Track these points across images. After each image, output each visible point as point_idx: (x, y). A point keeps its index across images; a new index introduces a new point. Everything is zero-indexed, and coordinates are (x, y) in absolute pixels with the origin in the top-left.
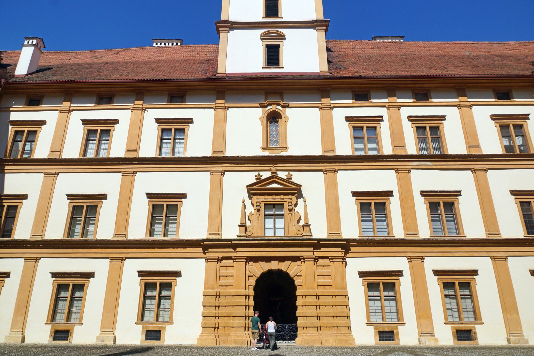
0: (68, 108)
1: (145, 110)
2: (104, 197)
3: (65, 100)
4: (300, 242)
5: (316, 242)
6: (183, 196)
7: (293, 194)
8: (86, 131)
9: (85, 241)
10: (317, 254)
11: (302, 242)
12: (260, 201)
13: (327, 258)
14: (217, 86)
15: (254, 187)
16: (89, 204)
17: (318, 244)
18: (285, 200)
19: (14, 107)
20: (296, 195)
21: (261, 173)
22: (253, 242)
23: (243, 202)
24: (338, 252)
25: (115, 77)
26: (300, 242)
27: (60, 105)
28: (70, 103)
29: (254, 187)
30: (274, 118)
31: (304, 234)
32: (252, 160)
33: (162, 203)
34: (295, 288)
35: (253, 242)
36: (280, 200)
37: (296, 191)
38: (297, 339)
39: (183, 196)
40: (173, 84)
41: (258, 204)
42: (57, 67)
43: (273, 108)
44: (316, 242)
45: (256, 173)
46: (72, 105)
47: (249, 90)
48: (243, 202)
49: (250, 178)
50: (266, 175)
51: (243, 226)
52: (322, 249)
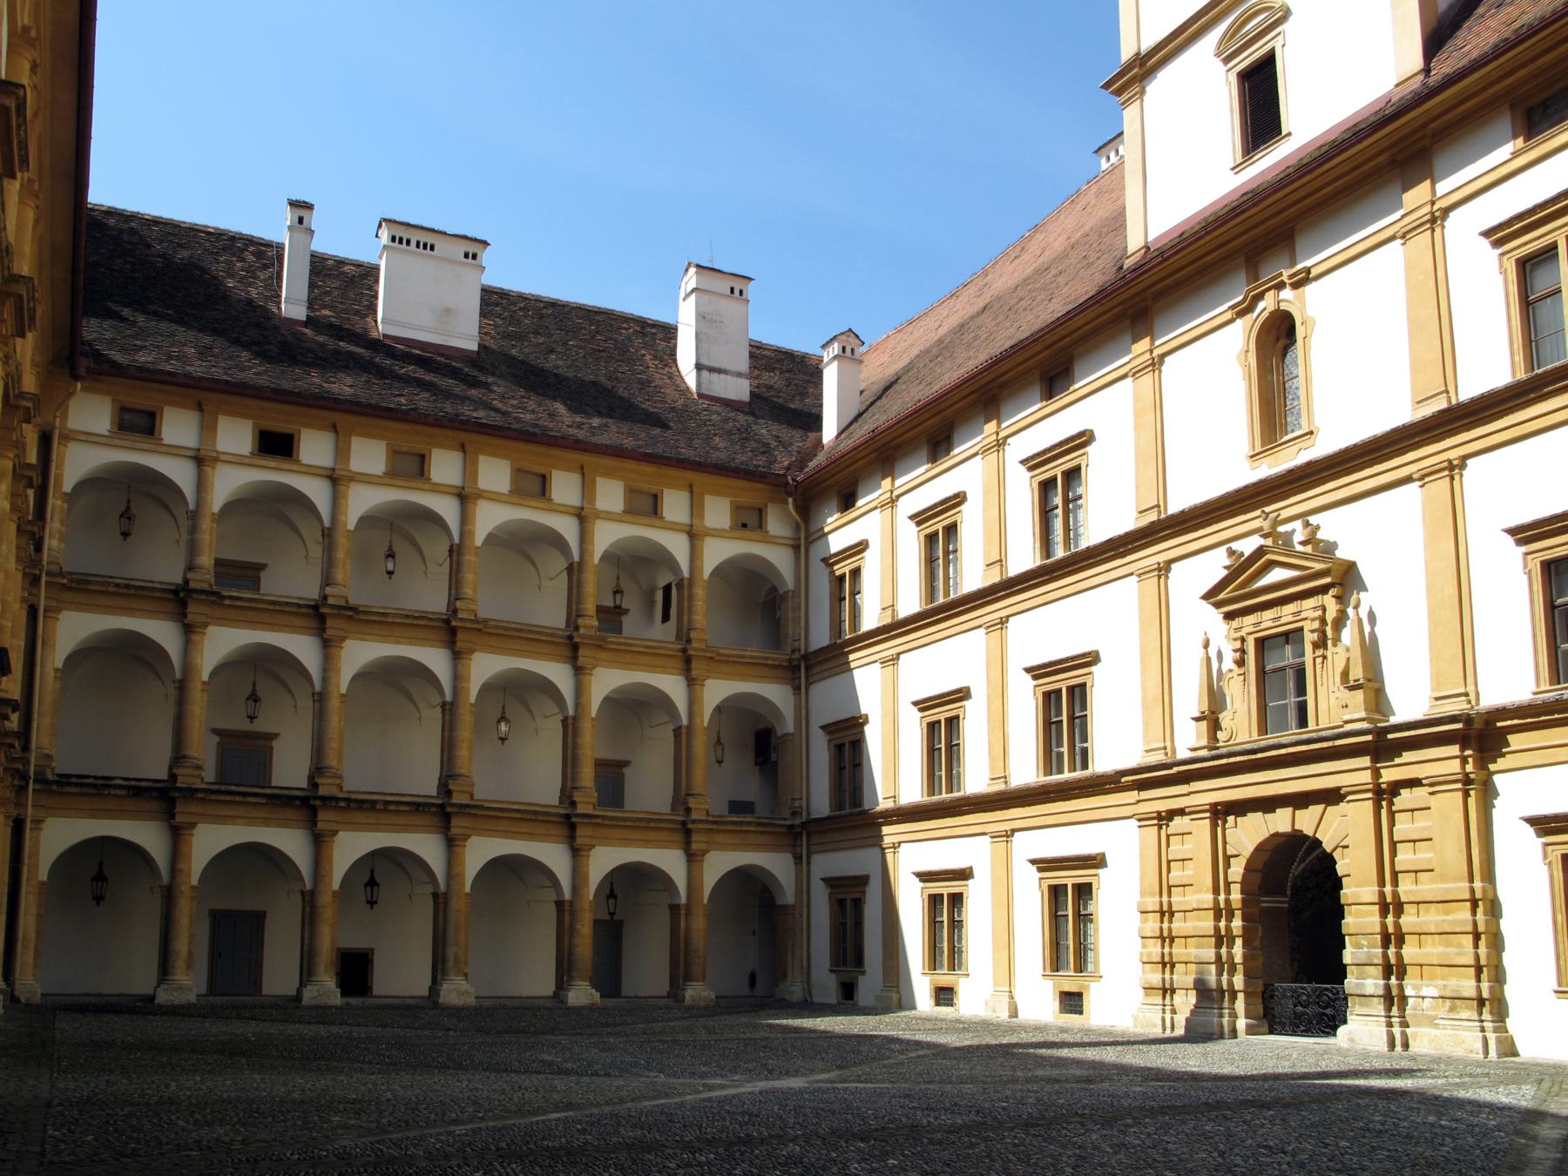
0: (1147, 356)
1: (1004, 444)
2: (962, 694)
3: (1135, 341)
4: (1325, 745)
5: (1369, 738)
6: (1091, 659)
7: (1323, 590)
8: (1035, 485)
9: (958, 799)
10: (1389, 775)
11: (1330, 744)
12: (1243, 633)
13: (1414, 783)
14: (1126, 300)
15: (1221, 596)
16: (948, 715)
17: (1383, 744)
18: (1303, 615)
19: (832, 520)
20: (1332, 592)
21: (1235, 546)
22: (1232, 760)
23: (1206, 646)
24: (1445, 761)
25: (1056, 308)
26: (1325, 745)
27: (979, 439)
28: (1148, 339)
29: (1221, 596)
30: (1279, 335)
31: (1346, 717)
32: (1232, 504)
33: (1056, 686)
34: (1337, 884)
35: (1232, 760)
36: (1290, 618)
37: (1328, 580)
38: (1341, 1030)
39: (1091, 659)
40: (1038, 347)
41: (1238, 645)
42: (908, 369)
43: (1267, 305)
44: (1369, 738)
45: (1224, 548)
46: (898, 483)
47: (1178, 285)
48: (1206, 646)
49: (1214, 566)
50: (1248, 546)
51: (1211, 720)
52: (1408, 756)
